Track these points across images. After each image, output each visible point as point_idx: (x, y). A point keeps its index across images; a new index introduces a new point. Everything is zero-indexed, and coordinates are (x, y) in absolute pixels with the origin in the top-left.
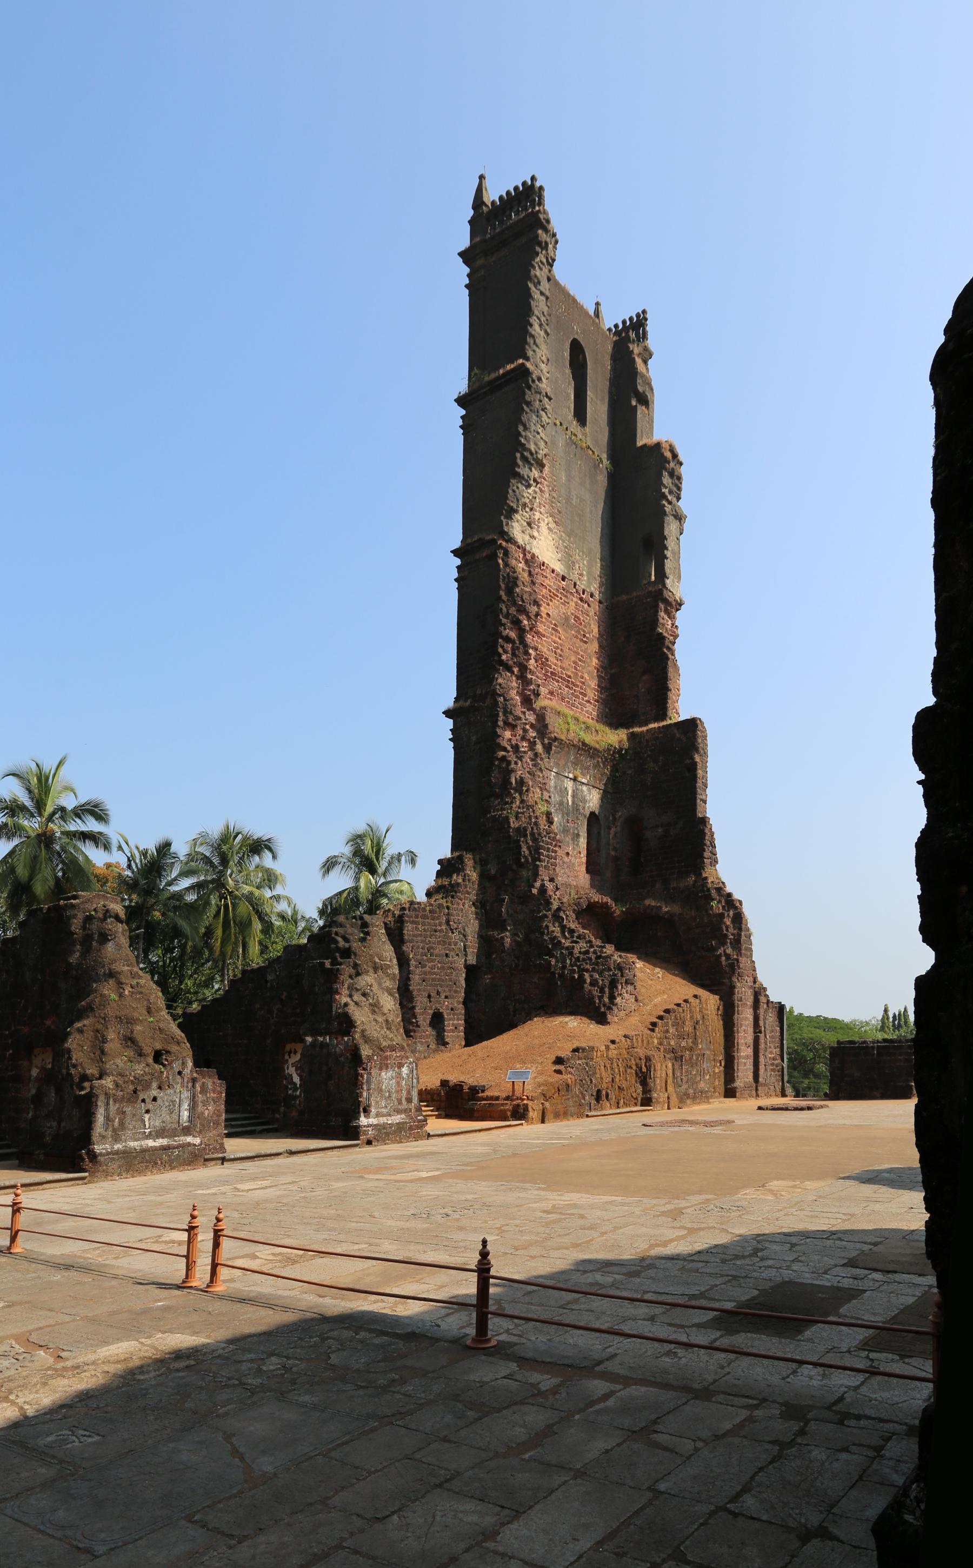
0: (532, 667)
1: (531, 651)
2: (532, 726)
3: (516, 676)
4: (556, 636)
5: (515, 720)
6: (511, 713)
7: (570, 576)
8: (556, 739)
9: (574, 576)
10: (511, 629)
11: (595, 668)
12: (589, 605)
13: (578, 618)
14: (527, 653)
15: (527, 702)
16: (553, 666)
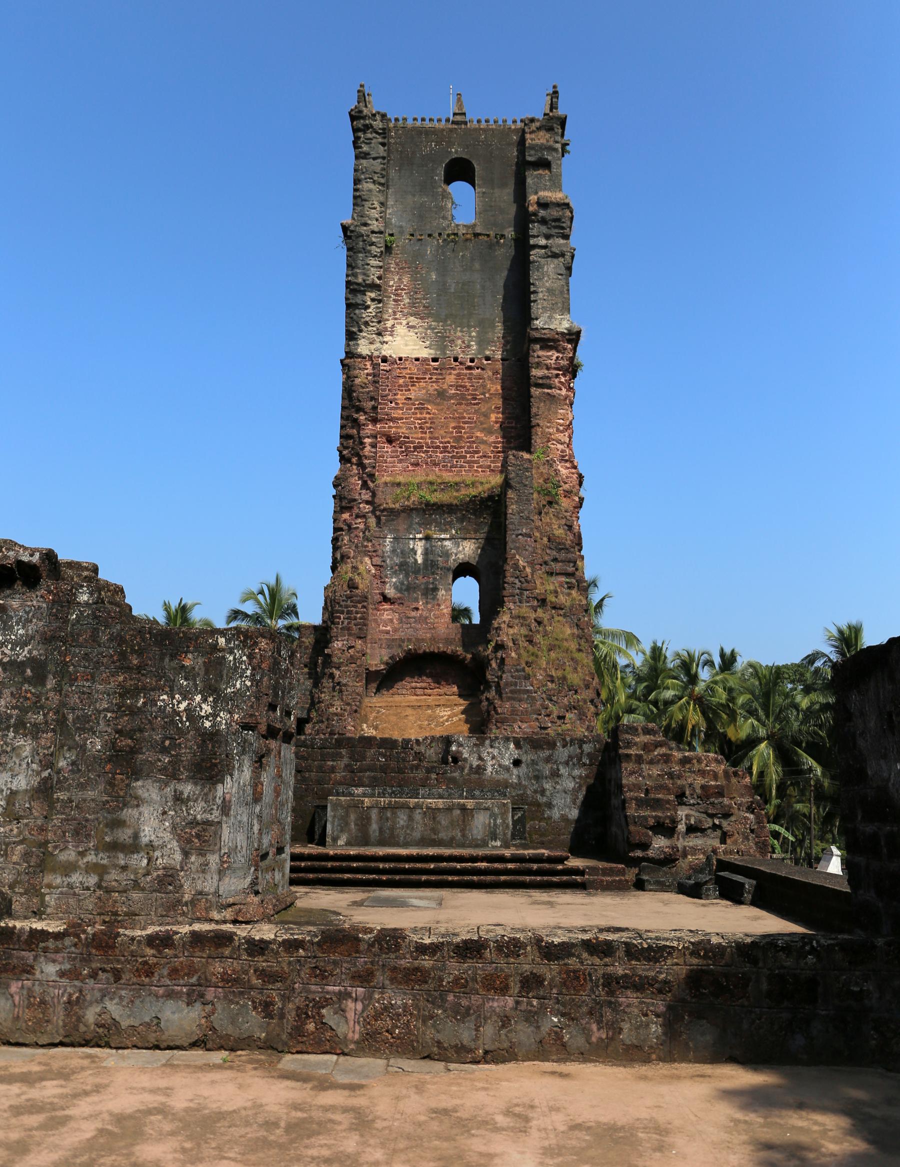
0: (367, 454)
1: (367, 441)
2: (367, 502)
3: (356, 464)
4: (421, 413)
5: (349, 502)
6: (345, 498)
7: (445, 354)
8: (385, 510)
9: (457, 350)
10: (353, 427)
11: (496, 422)
12: (483, 369)
13: (461, 386)
14: (362, 443)
15: (365, 485)
16: (417, 441)
